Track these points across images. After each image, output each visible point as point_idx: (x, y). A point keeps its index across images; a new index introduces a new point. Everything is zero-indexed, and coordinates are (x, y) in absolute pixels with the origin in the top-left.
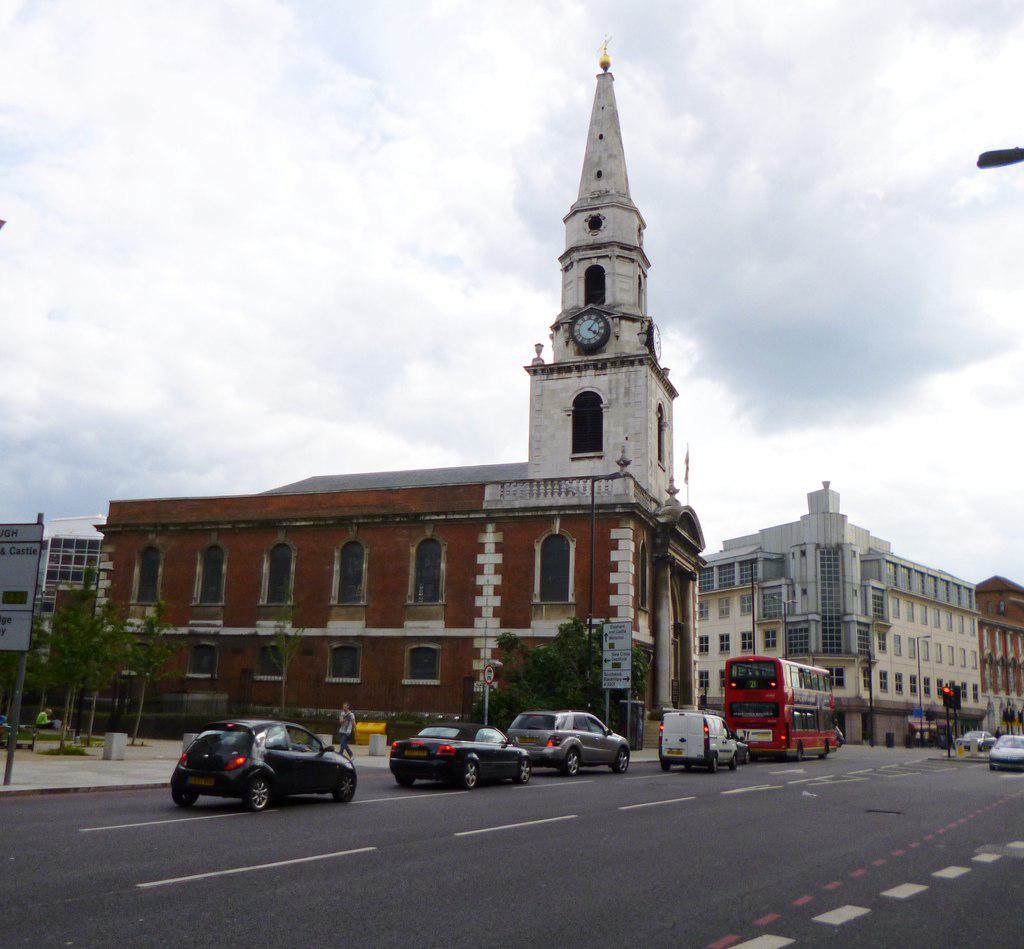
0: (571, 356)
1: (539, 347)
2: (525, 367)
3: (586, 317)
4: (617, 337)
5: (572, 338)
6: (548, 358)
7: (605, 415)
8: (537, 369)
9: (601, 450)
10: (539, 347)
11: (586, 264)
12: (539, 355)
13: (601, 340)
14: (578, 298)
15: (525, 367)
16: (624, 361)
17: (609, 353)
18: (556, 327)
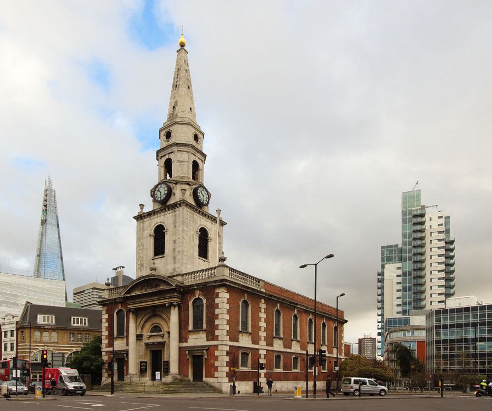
0: (157, 206)
1: (142, 206)
2: (133, 217)
3: (159, 186)
4: (174, 194)
5: (155, 201)
6: (146, 210)
7: (166, 236)
8: (140, 218)
9: (163, 253)
10: (142, 206)
11: (164, 159)
12: (142, 209)
13: (165, 198)
14: (163, 177)
15: (133, 217)
16: (175, 206)
17: (172, 201)
18: (152, 196)
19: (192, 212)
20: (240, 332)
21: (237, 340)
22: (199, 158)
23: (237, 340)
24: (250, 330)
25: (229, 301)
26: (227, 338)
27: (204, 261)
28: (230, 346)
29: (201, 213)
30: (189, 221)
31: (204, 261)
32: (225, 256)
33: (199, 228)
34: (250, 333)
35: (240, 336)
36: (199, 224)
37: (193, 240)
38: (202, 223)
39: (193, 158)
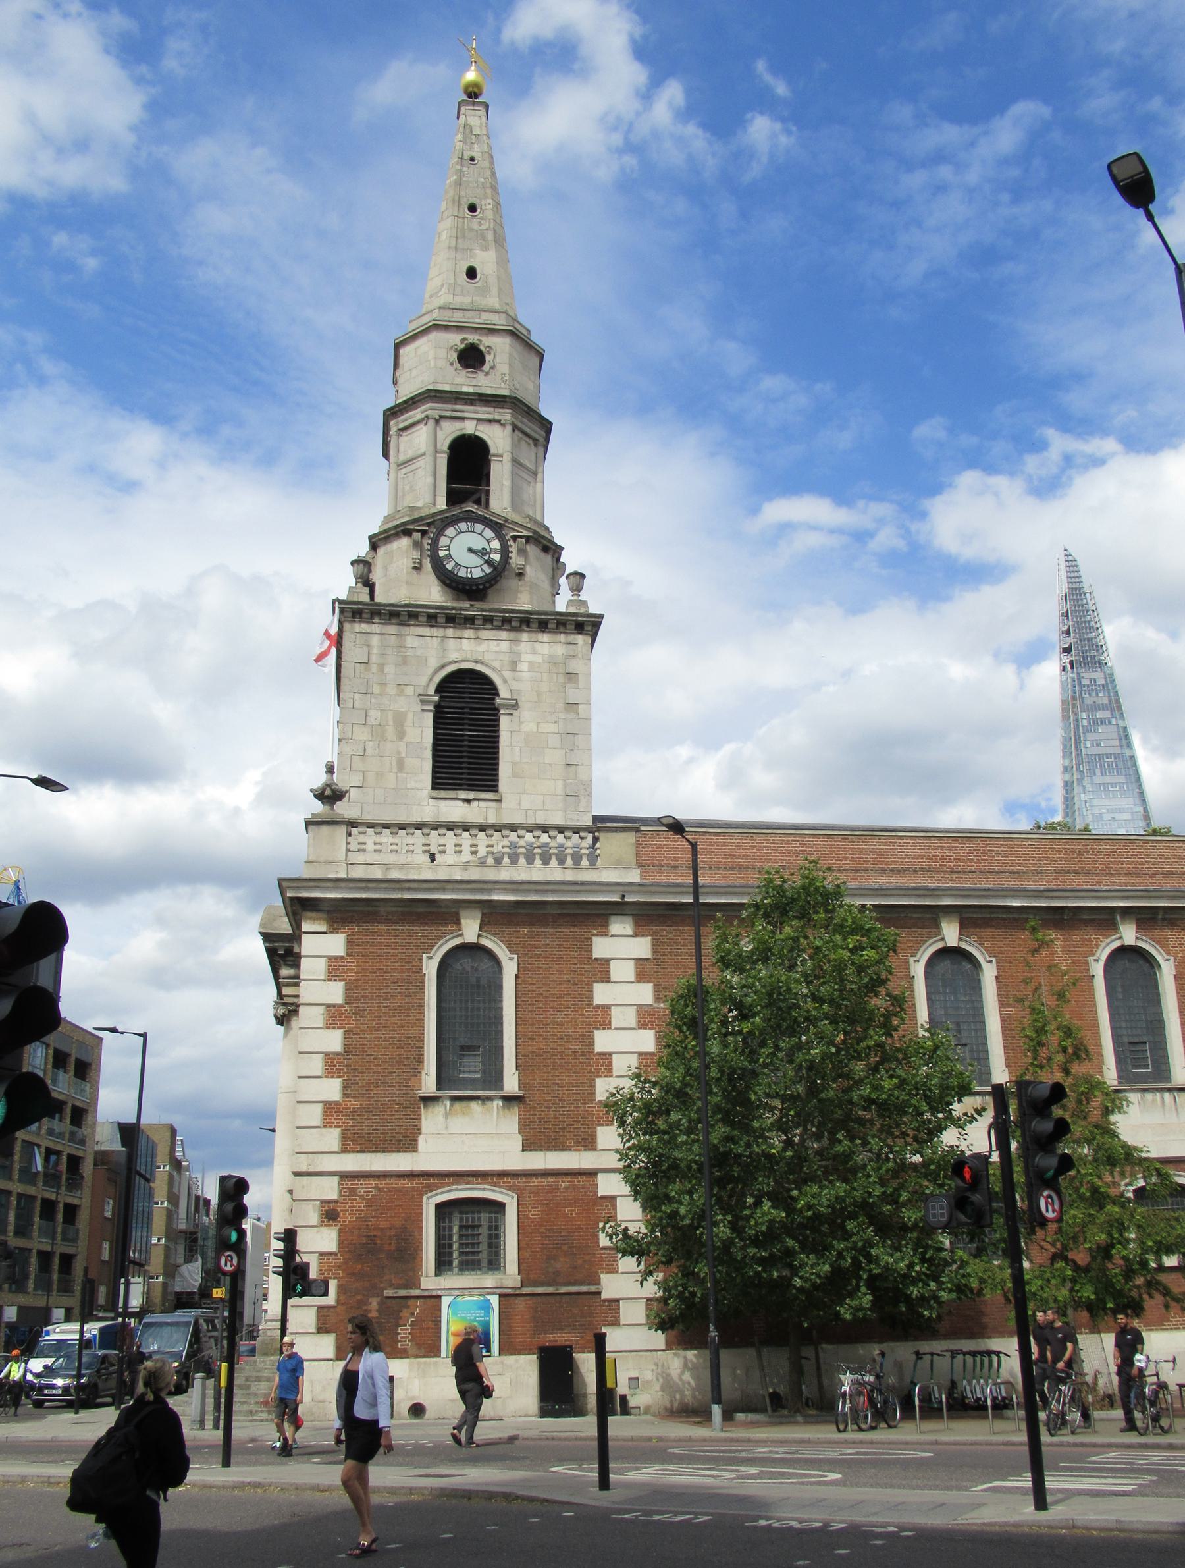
19: (392, 629)
20: (428, 1100)
21: (408, 1144)
22: (478, 420)
23: (408, 1144)
24: (511, 1083)
25: (335, 970)
26: (332, 1138)
27: (468, 801)
28: (344, 1176)
29: (441, 620)
30: (374, 669)
31: (468, 801)
32: (340, 780)
33: (438, 679)
34: (509, 1100)
35: (432, 1121)
36: (433, 663)
37: (401, 735)
38: (454, 656)
39: (449, 432)
